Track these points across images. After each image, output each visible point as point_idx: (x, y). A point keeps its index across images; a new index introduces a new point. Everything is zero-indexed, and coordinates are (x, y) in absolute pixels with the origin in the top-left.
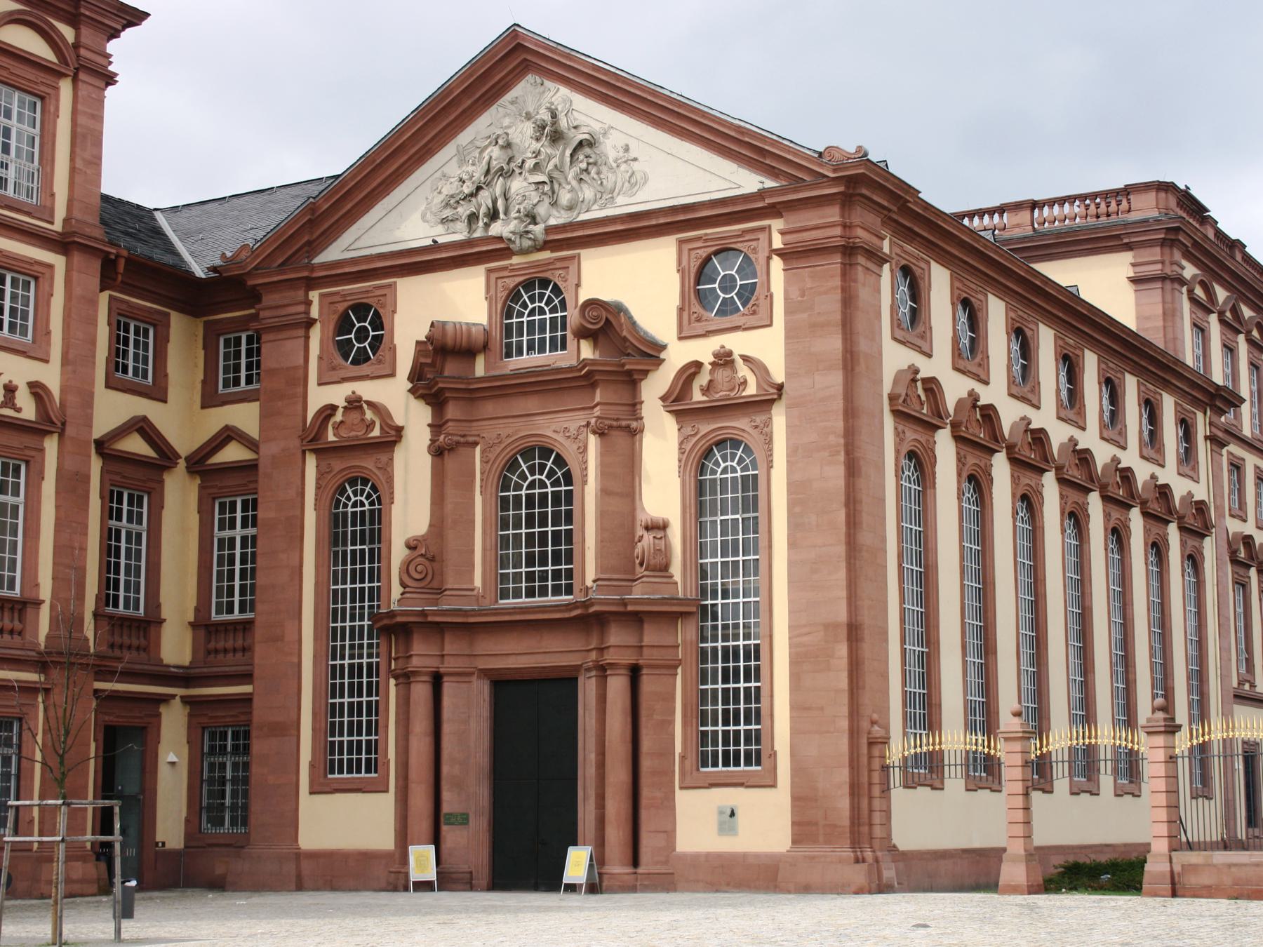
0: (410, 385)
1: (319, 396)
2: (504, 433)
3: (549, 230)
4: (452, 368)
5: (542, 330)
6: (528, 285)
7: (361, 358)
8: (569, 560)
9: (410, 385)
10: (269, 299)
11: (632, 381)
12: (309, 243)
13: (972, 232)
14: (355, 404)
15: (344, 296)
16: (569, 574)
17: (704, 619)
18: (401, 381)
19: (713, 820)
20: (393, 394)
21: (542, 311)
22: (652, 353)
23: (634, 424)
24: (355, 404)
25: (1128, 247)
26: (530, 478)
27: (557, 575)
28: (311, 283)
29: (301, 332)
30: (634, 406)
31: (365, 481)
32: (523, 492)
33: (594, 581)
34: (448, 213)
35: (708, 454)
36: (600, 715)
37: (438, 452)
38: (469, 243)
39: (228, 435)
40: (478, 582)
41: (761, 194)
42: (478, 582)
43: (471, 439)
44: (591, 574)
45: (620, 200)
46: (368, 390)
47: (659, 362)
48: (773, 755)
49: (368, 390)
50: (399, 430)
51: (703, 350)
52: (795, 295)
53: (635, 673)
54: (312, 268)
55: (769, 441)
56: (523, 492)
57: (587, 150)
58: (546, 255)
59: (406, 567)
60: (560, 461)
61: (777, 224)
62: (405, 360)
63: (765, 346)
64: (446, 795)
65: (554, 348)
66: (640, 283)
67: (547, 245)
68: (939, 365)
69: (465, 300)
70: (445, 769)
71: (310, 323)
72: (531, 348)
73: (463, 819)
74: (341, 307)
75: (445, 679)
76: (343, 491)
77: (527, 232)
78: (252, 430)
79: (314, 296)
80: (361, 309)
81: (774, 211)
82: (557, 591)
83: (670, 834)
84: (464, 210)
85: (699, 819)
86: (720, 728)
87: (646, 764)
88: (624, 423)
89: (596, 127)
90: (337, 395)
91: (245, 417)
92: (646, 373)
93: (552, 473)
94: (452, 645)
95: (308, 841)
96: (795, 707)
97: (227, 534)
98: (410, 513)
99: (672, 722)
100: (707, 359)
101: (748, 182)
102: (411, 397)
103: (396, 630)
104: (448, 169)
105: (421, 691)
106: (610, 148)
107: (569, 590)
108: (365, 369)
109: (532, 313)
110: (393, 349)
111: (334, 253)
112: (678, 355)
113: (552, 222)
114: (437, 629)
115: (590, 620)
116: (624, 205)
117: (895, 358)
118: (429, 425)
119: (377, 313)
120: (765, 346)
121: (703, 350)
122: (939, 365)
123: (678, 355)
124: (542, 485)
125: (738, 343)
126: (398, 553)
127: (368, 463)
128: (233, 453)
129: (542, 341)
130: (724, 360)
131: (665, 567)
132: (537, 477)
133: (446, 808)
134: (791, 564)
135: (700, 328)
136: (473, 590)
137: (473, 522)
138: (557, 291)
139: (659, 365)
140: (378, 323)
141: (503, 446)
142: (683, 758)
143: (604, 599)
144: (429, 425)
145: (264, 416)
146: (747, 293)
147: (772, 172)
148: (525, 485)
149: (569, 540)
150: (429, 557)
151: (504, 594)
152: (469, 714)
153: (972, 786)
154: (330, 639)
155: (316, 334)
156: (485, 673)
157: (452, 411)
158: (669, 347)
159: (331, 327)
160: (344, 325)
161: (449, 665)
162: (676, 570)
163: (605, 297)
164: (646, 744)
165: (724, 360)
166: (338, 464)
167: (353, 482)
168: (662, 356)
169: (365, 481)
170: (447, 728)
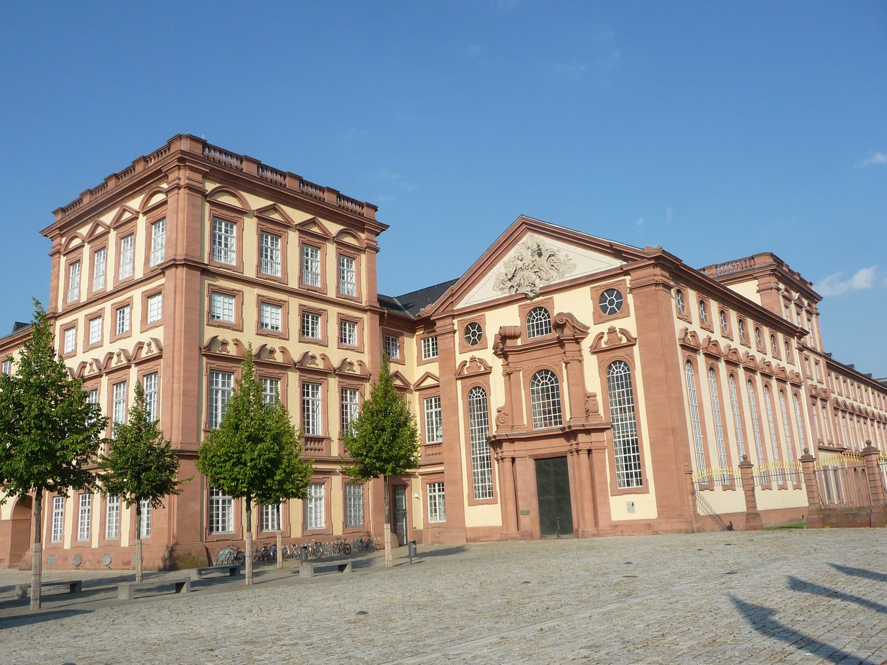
1: (460, 358)
3: (541, 288)
4: (509, 343)
5: (542, 326)
6: (535, 310)
7: (474, 343)
8: (560, 412)
10: (438, 324)
11: (577, 341)
12: (452, 303)
13: (703, 276)
14: (473, 360)
15: (466, 320)
16: (560, 417)
17: (614, 430)
18: (490, 350)
19: (625, 508)
20: (487, 355)
22: (583, 331)
23: (580, 358)
24: (473, 360)
25: (755, 278)
27: (555, 417)
28: (453, 317)
29: (452, 335)
31: (620, 362)
34: (502, 286)
35: (610, 367)
36: (578, 469)
37: (508, 375)
38: (511, 296)
39: (428, 376)
40: (525, 422)
41: (621, 268)
42: (525, 422)
45: (567, 275)
46: (478, 354)
47: (587, 334)
48: (647, 481)
49: (478, 354)
51: (604, 328)
52: (638, 303)
53: (589, 451)
54: (453, 311)
55: (633, 361)
57: (553, 258)
58: (541, 298)
59: (498, 418)
60: (553, 375)
61: (628, 278)
62: (491, 342)
63: (628, 323)
64: (520, 504)
65: (546, 333)
66: (578, 305)
68: (695, 326)
69: (511, 317)
70: (519, 494)
71: (454, 332)
72: (538, 333)
73: (528, 513)
74: (465, 325)
76: (471, 392)
78: (437, 373)
79: (455, 321)
80: (473, 325)
81: (626, 273)
82: (556, 423)
83: (609, 514)
84: (509, 284)
85: (620, 508)
86: (633, 471)
87: (597, 487)
89: (555, 249)
90: (467, 357)
91: (434, 368)
93: (550, 379)
95: (470, 523)
96: (654, 461)
97: (430, 411)
98: (497, 398)
99: (605, 470)
100: (606, 331)
101: (617, 263)
103: (496, 443)
104: (500, 269)
105: (508, 463)
106: (561, 256)
107: (561, 423)
108: (476, 346)
110: (486, 338)
111: (461, 305)
112: (594, 331)
113: (541, 286)
115: (570, 434)
116: (568, 277)
117: (679, 325)
119: (479, 326)
120: (628, 323)
121: (604, 328)
122: (695, 326)
123: (594, 331)
125: (618, 324)
126: (494, 414)
127: (479, 381)
128: (430, 382)
129: (542, 330)
130: (612, 331)
131: (597, 411)
133: (521, 509)
134: (647, 407)
135: (602, 320)
138: (546, 311)
140: (480, 329)
142: (611, 483)
143: (576, 424)
145: (440, 367)
146: (619, 305)
147: (625, 259)
149: (559, 404)
150: (508, 413)
151: (536, 426)
152: (527, 472)
153: (725, 488)
154: (471, 446)
155: (457, 335)
156: (531, 456)
157: (511, 358)
159: (463, 332)
160: (467, 331)
162: (601, 411)
163: (565, 312)
164: (597, 480)
165: (612, 331)
166: (469, 382)
167: (475, 388)
169: (480, 388)
170: (519, 478)
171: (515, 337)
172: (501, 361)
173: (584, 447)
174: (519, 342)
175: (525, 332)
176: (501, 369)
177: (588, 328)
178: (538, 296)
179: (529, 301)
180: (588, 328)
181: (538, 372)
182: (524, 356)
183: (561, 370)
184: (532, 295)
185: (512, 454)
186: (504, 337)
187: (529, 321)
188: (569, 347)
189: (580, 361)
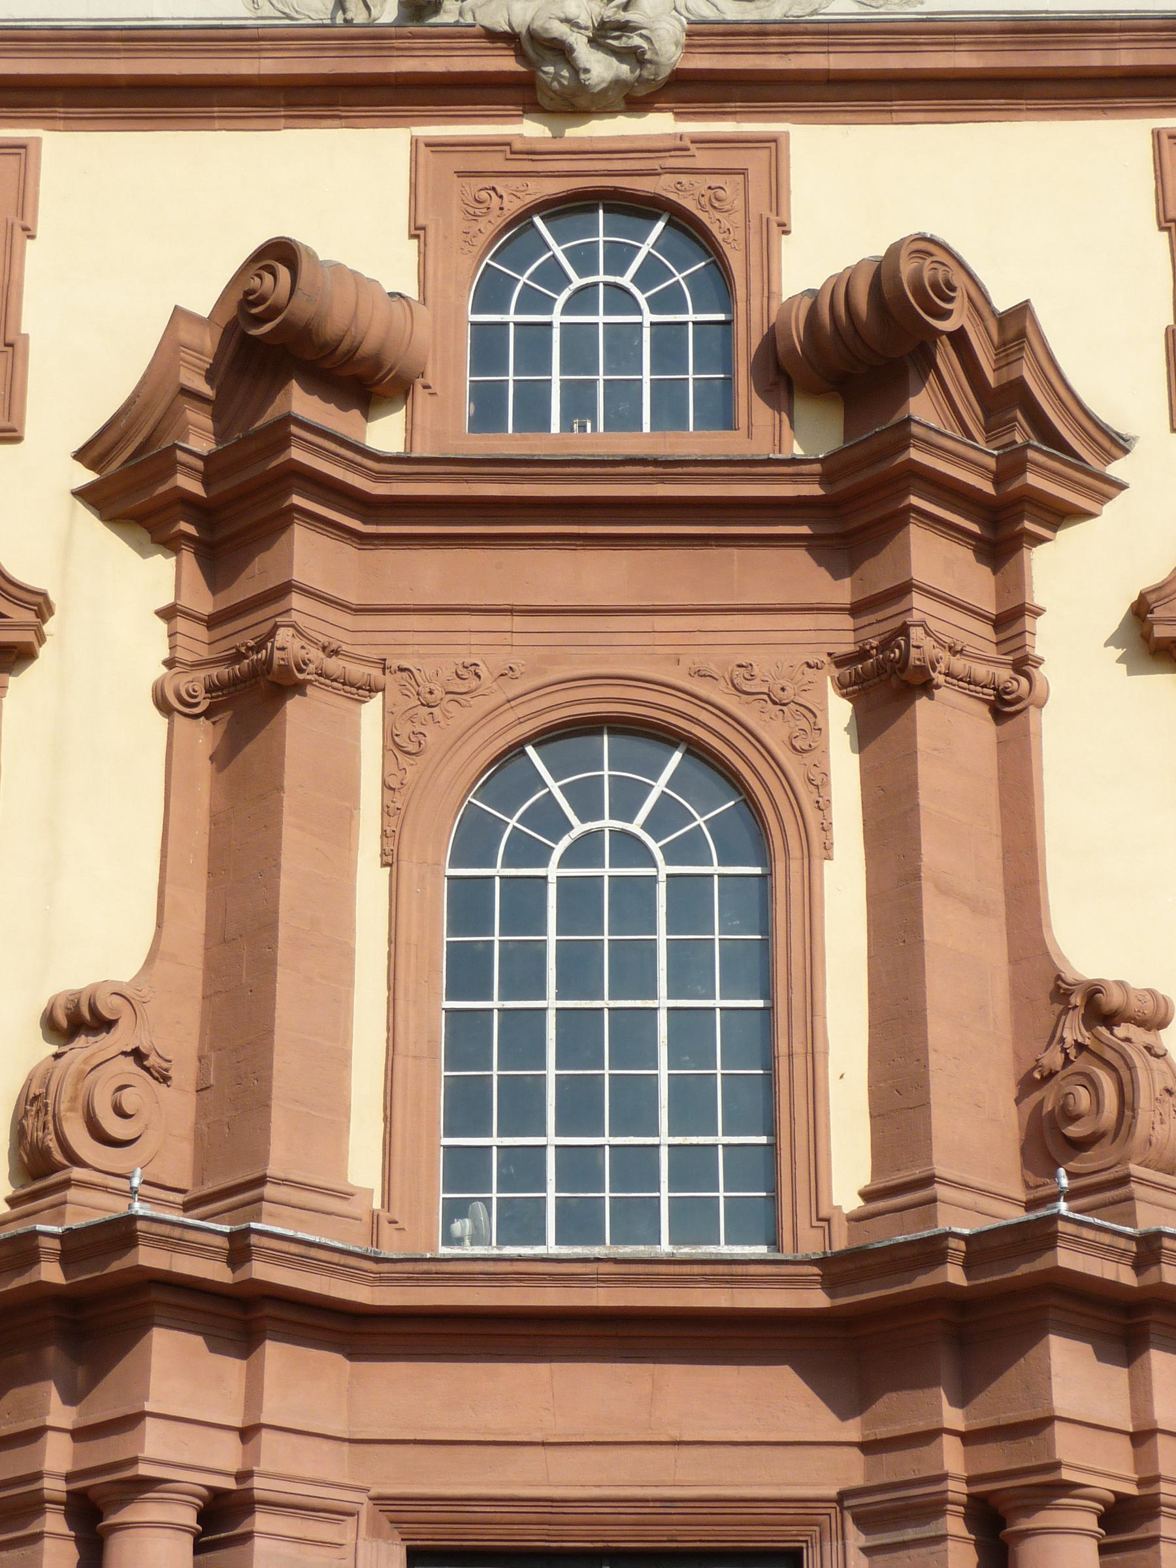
0: (86, 476)
2: (490, 662)
9: (86, 476)
11: (1004, 527)
21: (620, 299)
26: (579, 828)
30: (1011, 619)
32: (553, 871)
33: (868, 1196)
37: (239, 698)
42: (363, 1168)
43: (357, 671)
44: (849, 1170)
50: (41, 606)
56: (553, 871)
58: (658, 124)
67: (687, 89)
69: (352, 202)
72: (578, 402)
75: (261, 1521)
77: (625, 27)
88: (981, 671)
92: (1062, 515)
94: (300, 1381)
102: (88, 520)
109: (582, 300)
114: (242, 1317)
118: (168, 614)
124: (628, 848)
132: (607, 823)
136: (344, 1195)
137: (347, 954)
139: (1106, 498)
141: (481, 705)
144: (168, 614)
148: (559, 849)
156: (392, 1508)
157: (310, 555)
158: (1136, 449)
161: (280, 1465)
168: (1115, 470)
171: (367, 382)
172: (157, 576)
173: (1096, 1464)
174: (386, 433)
175: (452, 378)
176: (145, 651)
177: (1118, 445)
178: (634, 99)
179: (531, 129)
180: (1118, 445)
181: (544, 738)
182: (428, 573)
183: (809, 744)
184: (600, 68)
185: (220, 1459)
186: (275, 340)
187: (492, 292)
188: (934, 558)
189: (1005, 707)
